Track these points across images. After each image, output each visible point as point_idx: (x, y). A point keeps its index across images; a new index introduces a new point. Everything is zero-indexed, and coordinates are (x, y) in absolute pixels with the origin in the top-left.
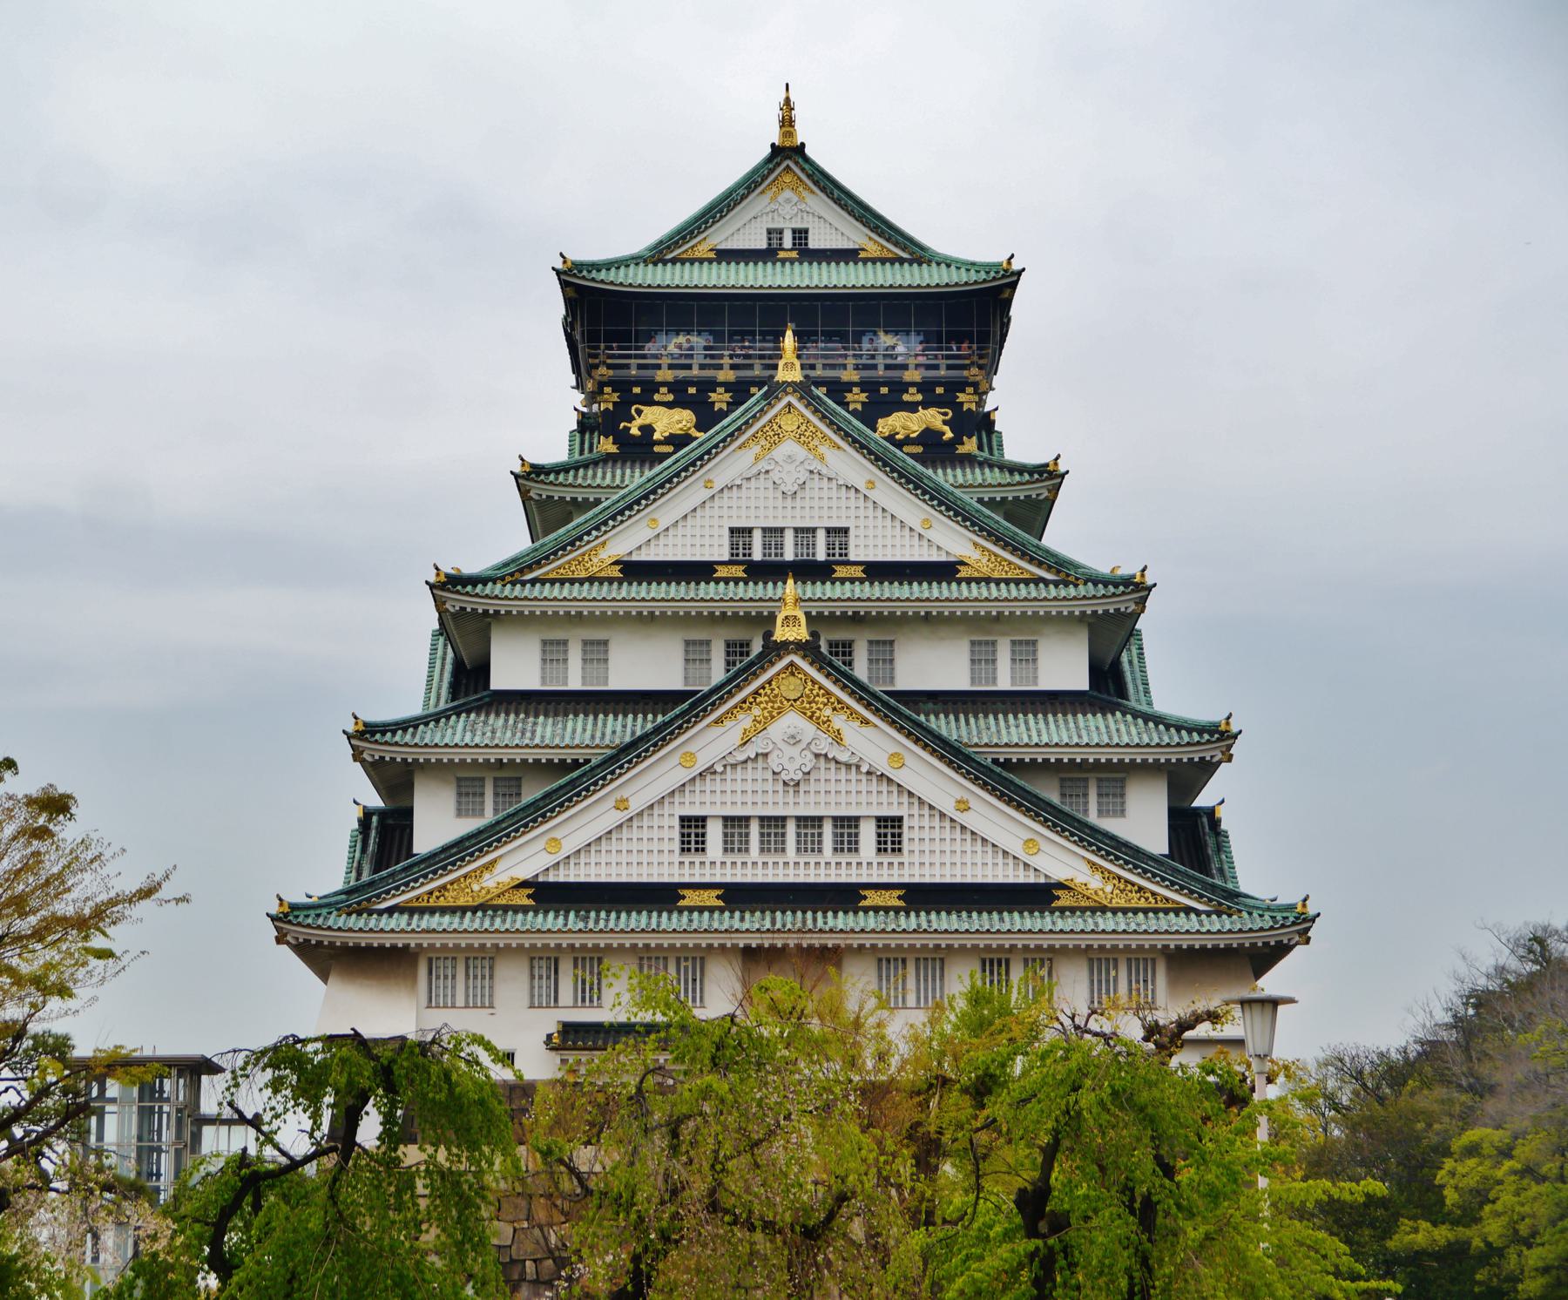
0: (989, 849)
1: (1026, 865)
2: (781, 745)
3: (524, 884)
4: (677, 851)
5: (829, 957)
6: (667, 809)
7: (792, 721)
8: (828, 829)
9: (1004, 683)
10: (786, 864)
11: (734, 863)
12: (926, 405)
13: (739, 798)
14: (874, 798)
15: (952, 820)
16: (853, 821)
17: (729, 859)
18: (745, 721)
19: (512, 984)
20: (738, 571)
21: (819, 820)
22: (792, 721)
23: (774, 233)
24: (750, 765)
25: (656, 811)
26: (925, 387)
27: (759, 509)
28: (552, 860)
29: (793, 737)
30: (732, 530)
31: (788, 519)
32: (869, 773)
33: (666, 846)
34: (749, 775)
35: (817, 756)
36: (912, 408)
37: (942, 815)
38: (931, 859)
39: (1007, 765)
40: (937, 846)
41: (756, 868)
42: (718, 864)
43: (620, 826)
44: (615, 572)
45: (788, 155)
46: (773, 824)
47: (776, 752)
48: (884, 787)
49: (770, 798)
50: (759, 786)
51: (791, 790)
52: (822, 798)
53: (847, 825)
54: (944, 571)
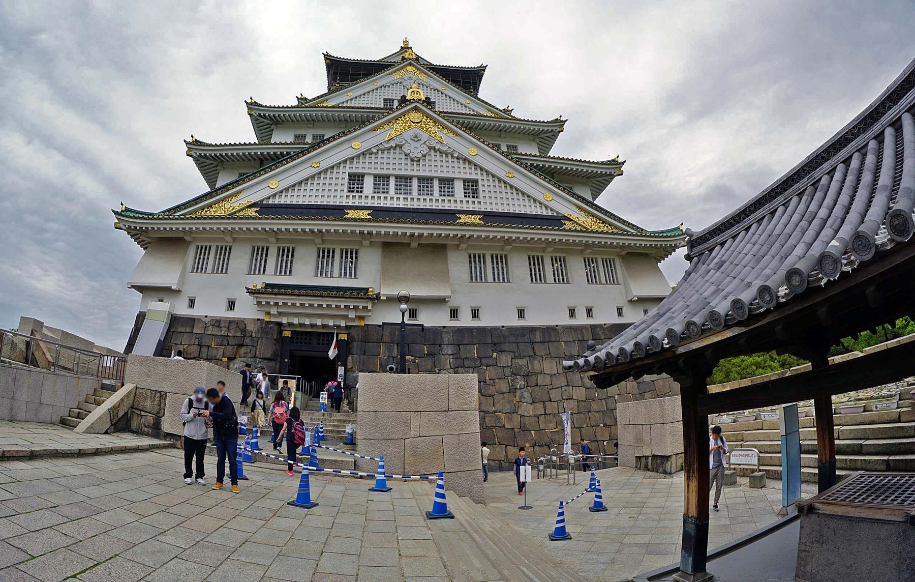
0: (526, 198)
1: (546, 207)
2: (409, 141)
3: (253, 205)
4: (346, 190)
6: (341, 170)
7: (415, 130)
8: (436, 183)
10: (412, 199)
11: (379, 198)
13: (385, 166)
14: (462, 170)
15: (505, 183)
16: (451, 180)
17: (376, 195)
19: (240, 259)
21: (430, 179)
24: (392, 151)
25: (335, 170)
27: (395, 94)
29: (416, 136)
30: (385, 100)
32: (458, 158)
33: (339, 188)
34: (392, 156)
35: (430, 148)
37: (500, 180)
40: (499, 195)
41: (393, 199)
43: (313, 177)
46: (404, 181)
47: (406, 146)
48: (467, 165)
49: (403, 167)
50: (397, 161)
51: (415, 163)
52: (433, 168)
53: (447, 183)
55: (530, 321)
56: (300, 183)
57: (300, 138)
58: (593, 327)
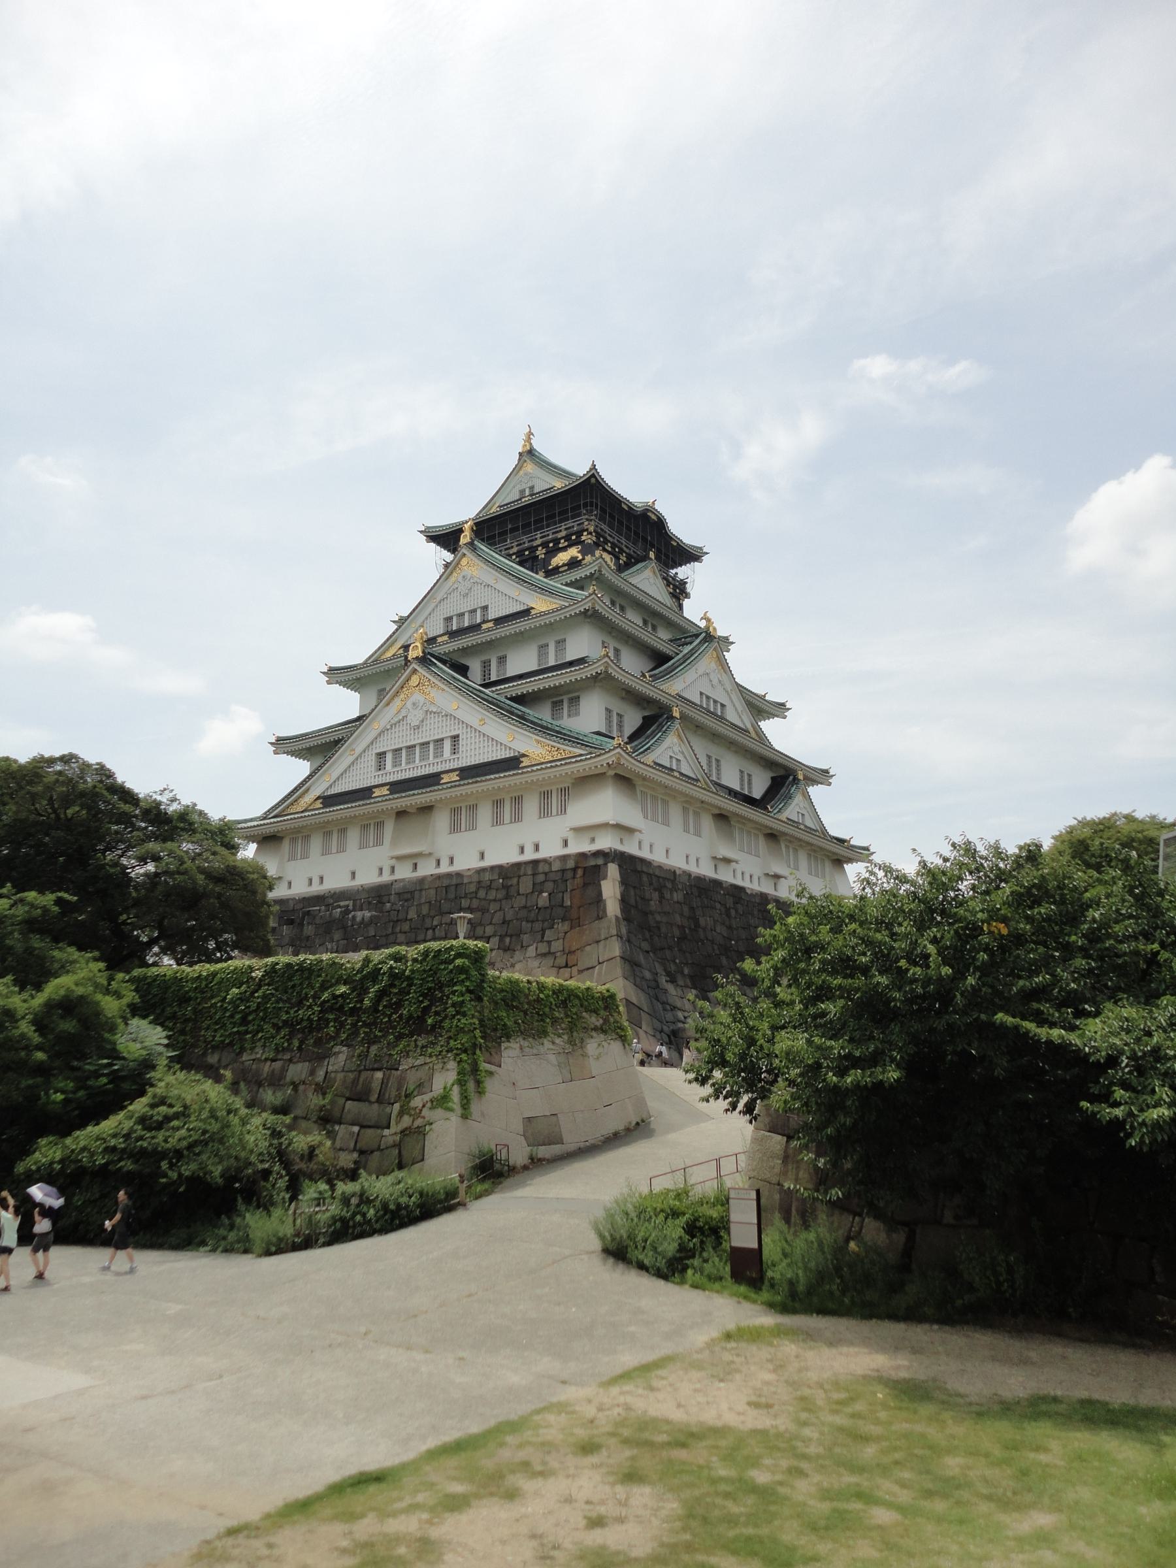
3: (318, 798)
5: (427, 810)
9: (552, 663)
12: (570, 546)
18: (397, 703)
20: (446, 638)
22: (417, 697)
23: (522, 492)
26: (567, 538)
28: (327, 784)
29: (414, 704)
31: (465, 607)
36: (565, 549)
38: (472, 754)
39: (512, 699)
42: (393, 773)
44: (401, 651)
45: (529, 453)
54: (526, 612)
55: (488, 862)
56: (345, 771)
57: (382, 693)
58: (535, 863)
